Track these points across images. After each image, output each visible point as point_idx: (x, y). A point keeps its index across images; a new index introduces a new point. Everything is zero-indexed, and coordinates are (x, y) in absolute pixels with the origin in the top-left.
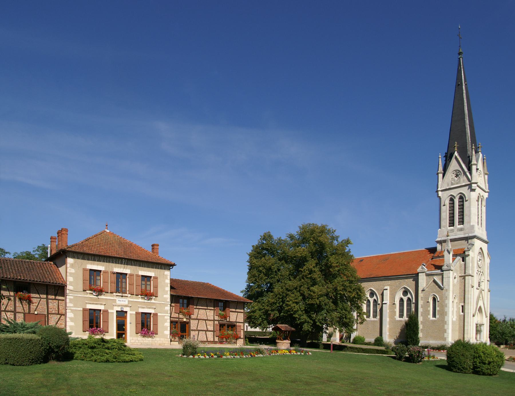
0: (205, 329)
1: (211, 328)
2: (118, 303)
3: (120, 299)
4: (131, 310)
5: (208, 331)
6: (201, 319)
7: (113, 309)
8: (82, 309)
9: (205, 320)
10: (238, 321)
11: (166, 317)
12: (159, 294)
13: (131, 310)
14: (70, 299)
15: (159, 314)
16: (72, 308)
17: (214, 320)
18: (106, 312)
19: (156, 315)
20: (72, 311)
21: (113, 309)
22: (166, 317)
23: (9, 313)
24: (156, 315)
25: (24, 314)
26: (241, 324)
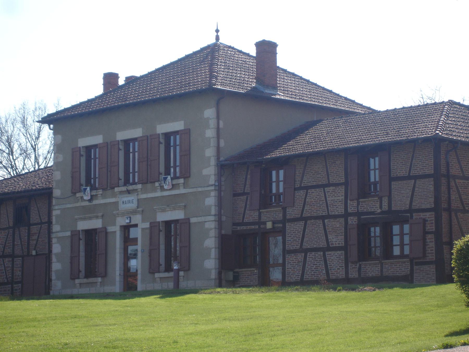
0: (323, 244)
1: (337, 240)
2: (122, 207)
3: (125, 199)
4: (143, 221)
5: (329, 248)
6: (311, 218)
7: (114, 224)
8: (68, 234)
9: (323, 218)
10: (416, 205)
11: (207, 225)
12: (194, 170)
13: (143, 221)
14: (57, 216)
15: (193, 220)
16: (61, 235)
17: (346, 215)
18: (104, 231)
19: (186, 222)
20: (60, 239)
21: (114, 224)
22: (207, 225)
23: (7, 259)
24: (186, 222)
25: (23, 257)
26: (428, 214)
